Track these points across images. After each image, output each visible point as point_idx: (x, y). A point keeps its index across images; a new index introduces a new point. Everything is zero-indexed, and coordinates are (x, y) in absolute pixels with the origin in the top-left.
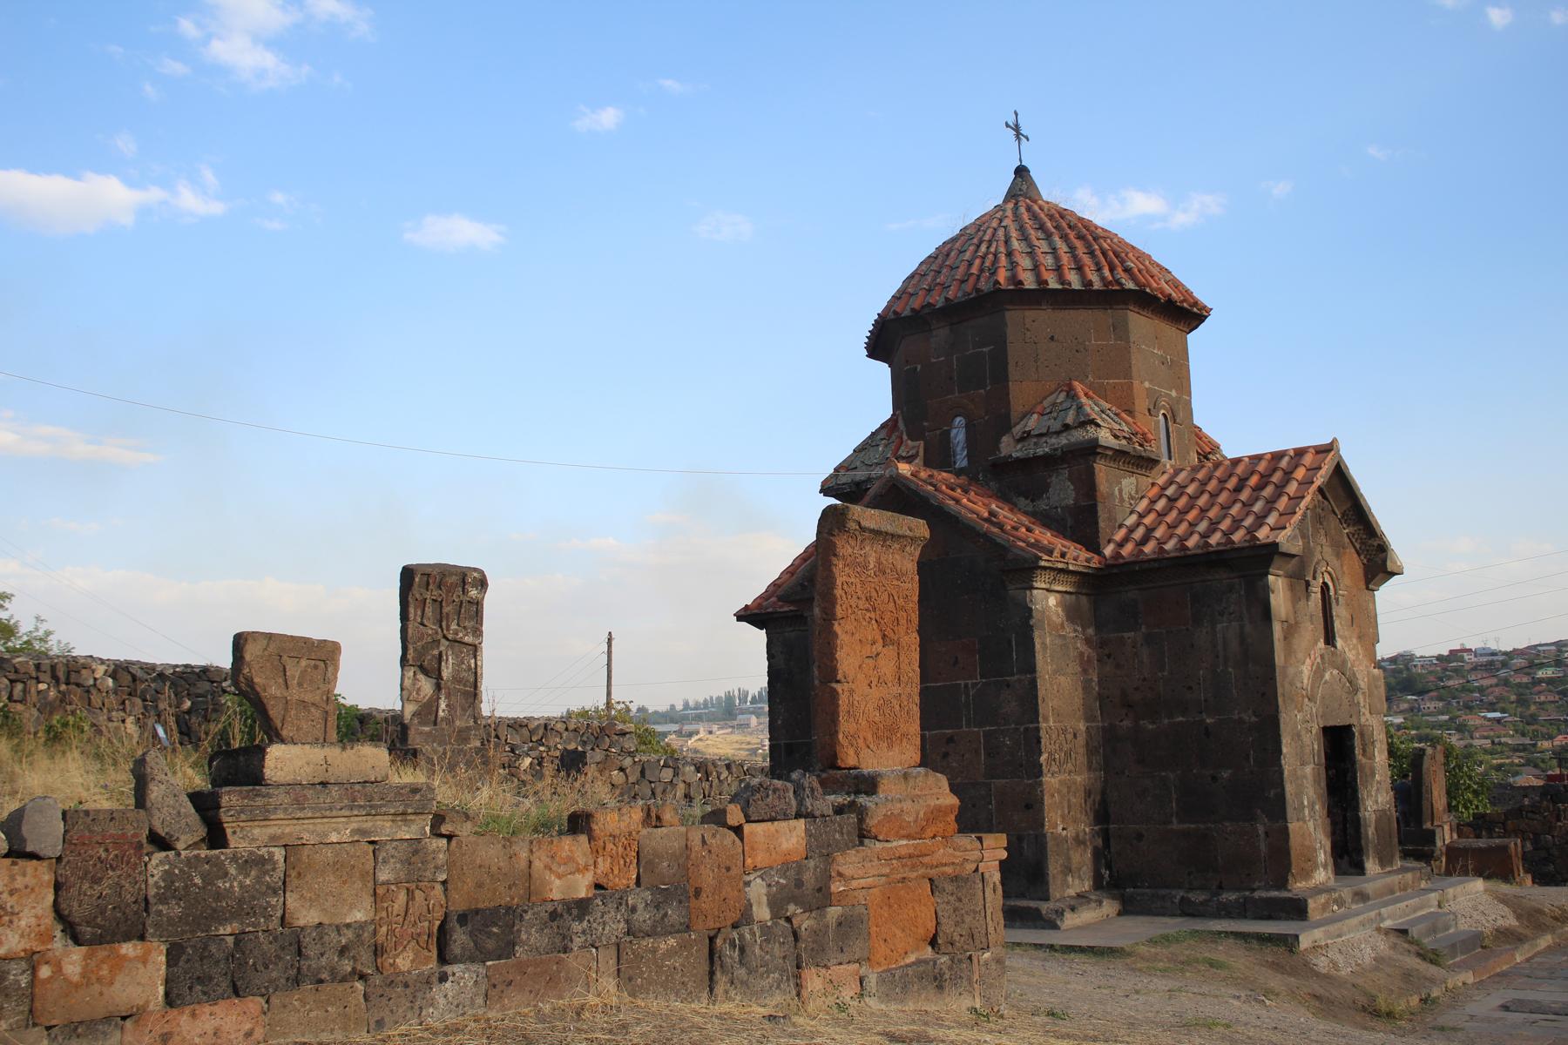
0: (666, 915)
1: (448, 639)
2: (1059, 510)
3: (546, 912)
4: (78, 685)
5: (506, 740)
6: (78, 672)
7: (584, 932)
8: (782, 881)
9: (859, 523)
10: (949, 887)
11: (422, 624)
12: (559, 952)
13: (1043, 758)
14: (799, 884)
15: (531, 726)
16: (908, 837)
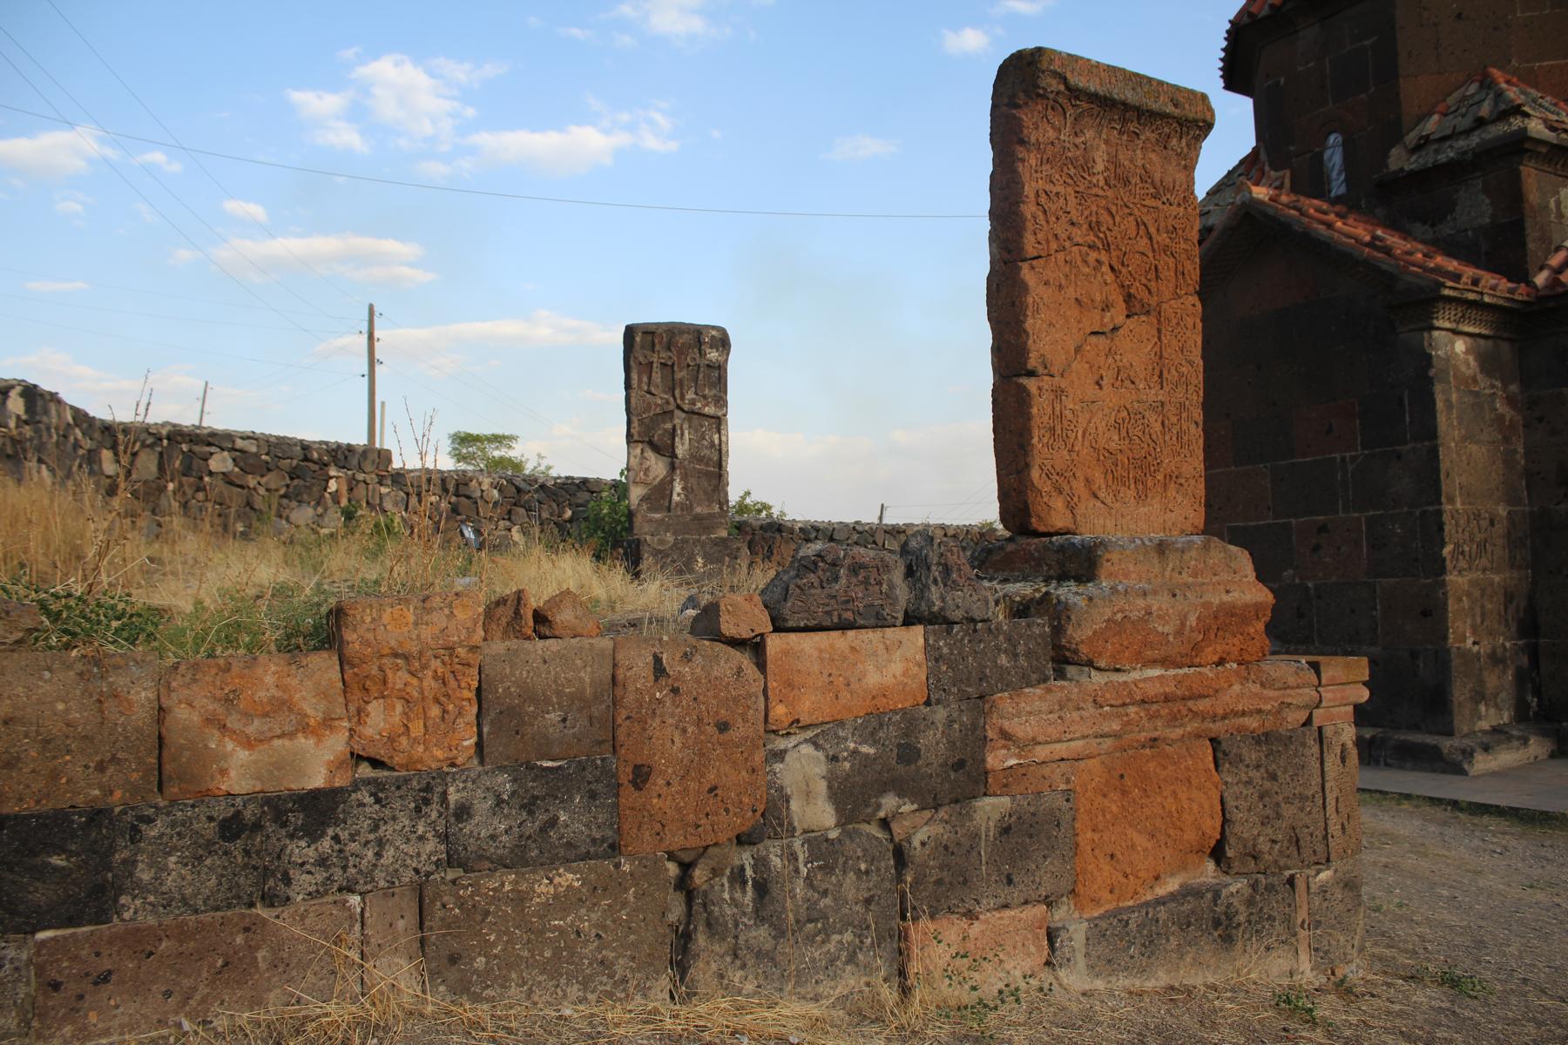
0: (553, 822)
1: (683, 410)
2: (1470, 233)
3: (211, 819)
4: (468, 497)
5: (884, 545)
6: (466, 485)
7: (322, 862)
8: (866, 749)
9: (1065, 80)
10: (1251, 755)
11: (649, 392)
12: (251, 905)
13: (1447, 551)
14: (908, 753)
15: (909, 532)
16: (1165, 662)
